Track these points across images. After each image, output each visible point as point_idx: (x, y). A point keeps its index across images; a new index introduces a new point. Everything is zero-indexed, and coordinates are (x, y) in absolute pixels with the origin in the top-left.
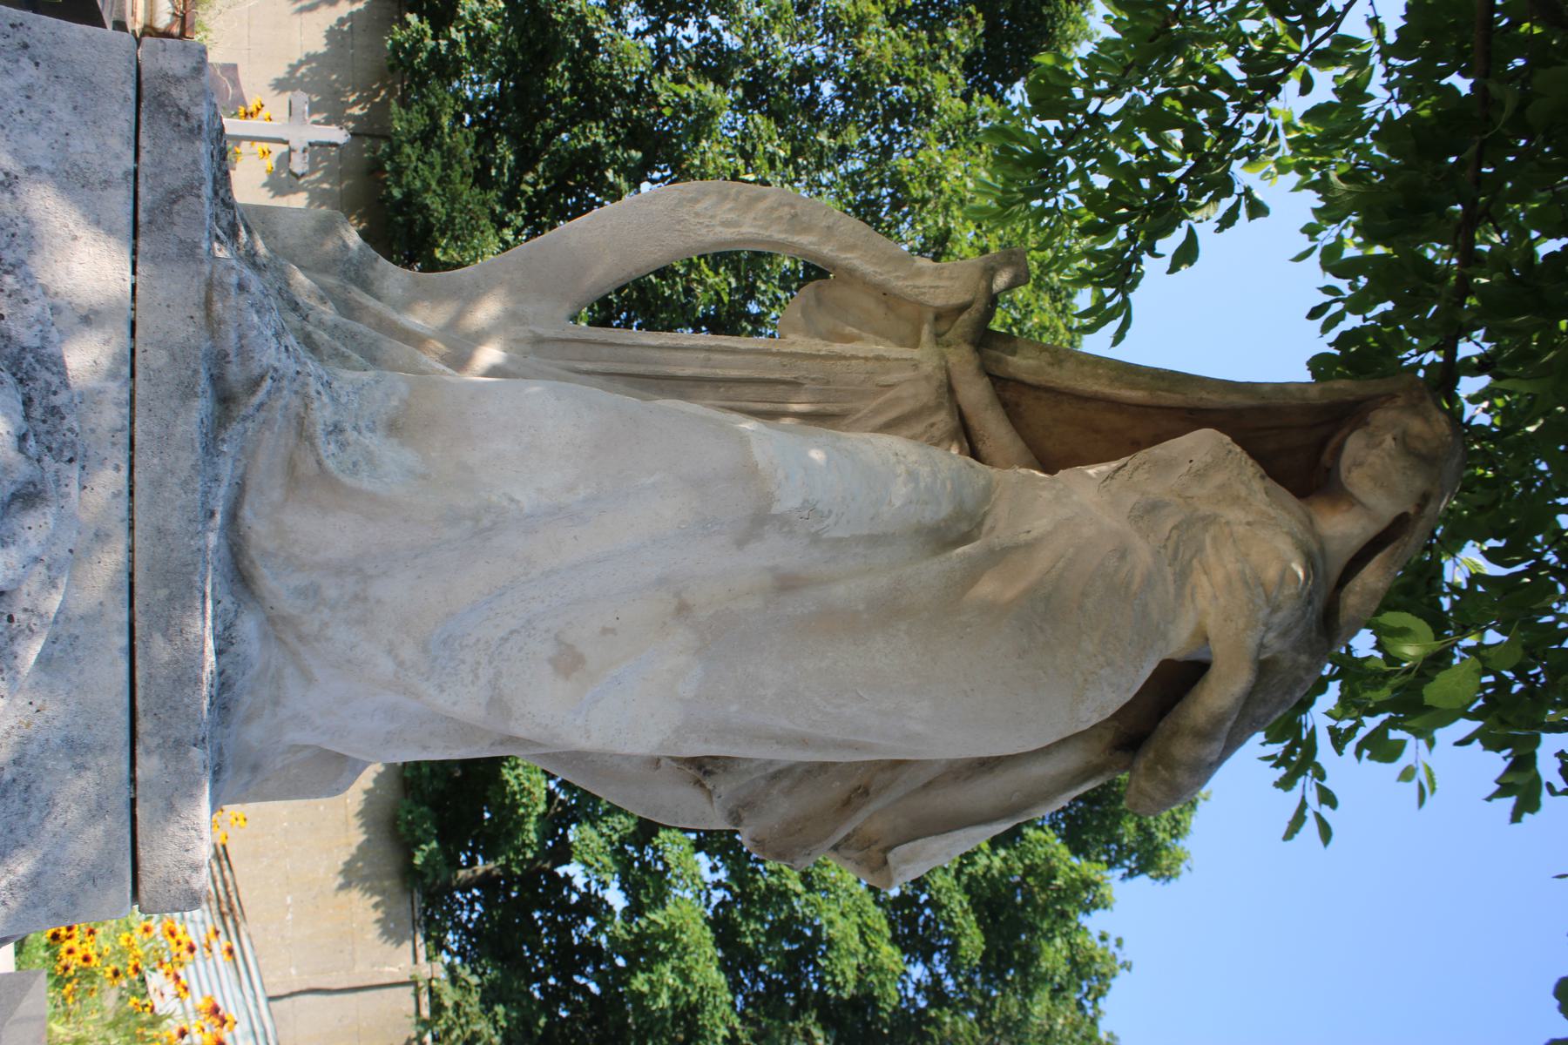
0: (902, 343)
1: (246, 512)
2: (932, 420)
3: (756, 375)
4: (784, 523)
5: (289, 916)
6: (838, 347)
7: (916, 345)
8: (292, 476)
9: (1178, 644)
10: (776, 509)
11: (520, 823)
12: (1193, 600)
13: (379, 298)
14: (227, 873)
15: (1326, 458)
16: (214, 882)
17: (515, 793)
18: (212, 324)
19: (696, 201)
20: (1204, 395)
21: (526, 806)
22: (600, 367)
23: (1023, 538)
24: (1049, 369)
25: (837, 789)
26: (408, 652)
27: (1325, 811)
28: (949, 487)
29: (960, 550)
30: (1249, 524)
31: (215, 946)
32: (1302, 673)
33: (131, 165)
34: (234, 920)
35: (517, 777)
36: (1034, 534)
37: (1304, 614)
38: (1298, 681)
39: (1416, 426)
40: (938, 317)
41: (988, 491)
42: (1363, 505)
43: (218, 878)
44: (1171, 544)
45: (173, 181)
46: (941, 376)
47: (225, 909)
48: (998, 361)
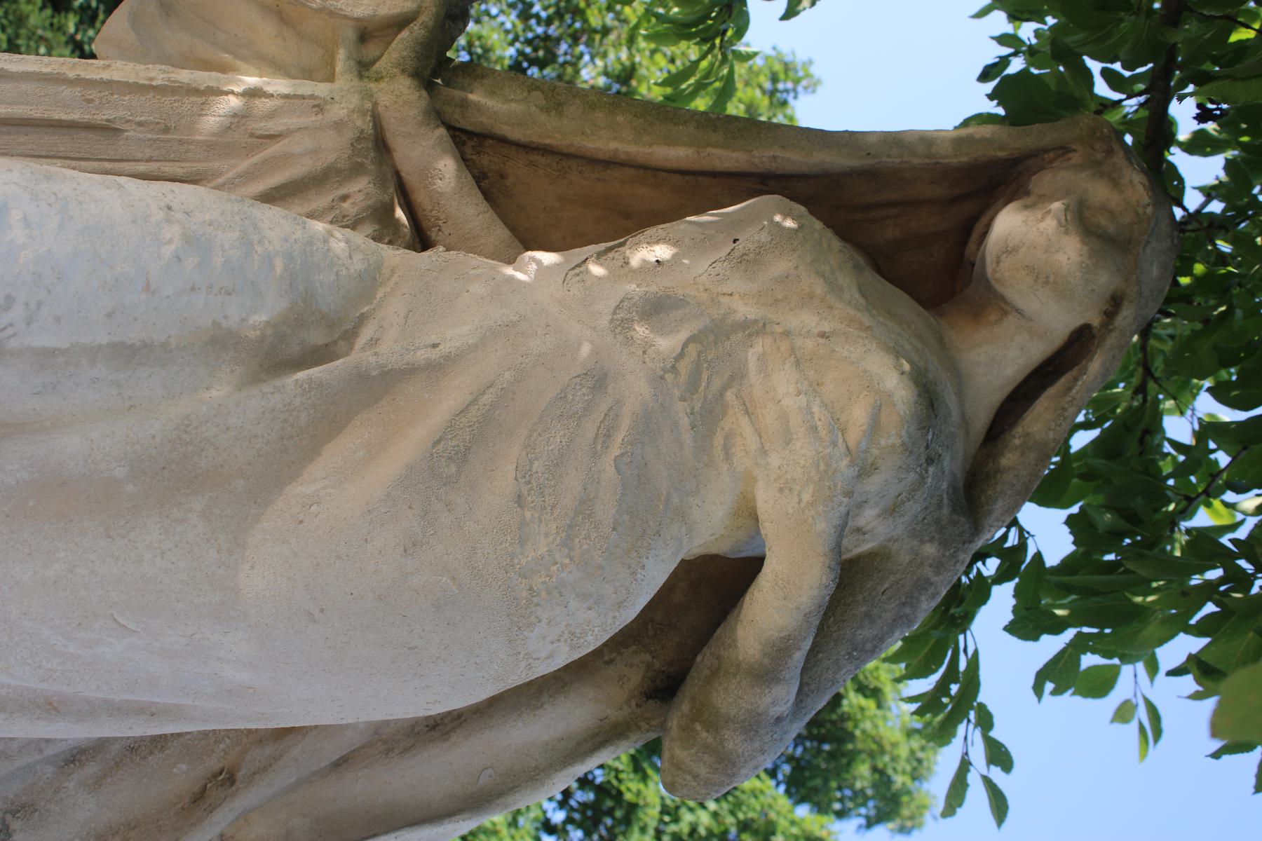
0: (308, 74)
2: (343, 191)
3: (36, 113)
6: (184, 76)
7: (331, 78)
9: (708, 530)
12: (728, 455)
15: (971, 247)
20: (779, 153)
23: (422, 355)
24: (543, 117)
25: (183, 776)
27: (996, 774)
28: (279, 264)
29: (301, 375)
30: (823, 335)
32: (928, 572)
36: (445, 348)
37: (922, 479)
38: (923, 585)
39: (1099, 192)
41: (369, 282)
42: (1018, 311)
44: (684, 367)
46: (366, 125)
48: (464, 105)
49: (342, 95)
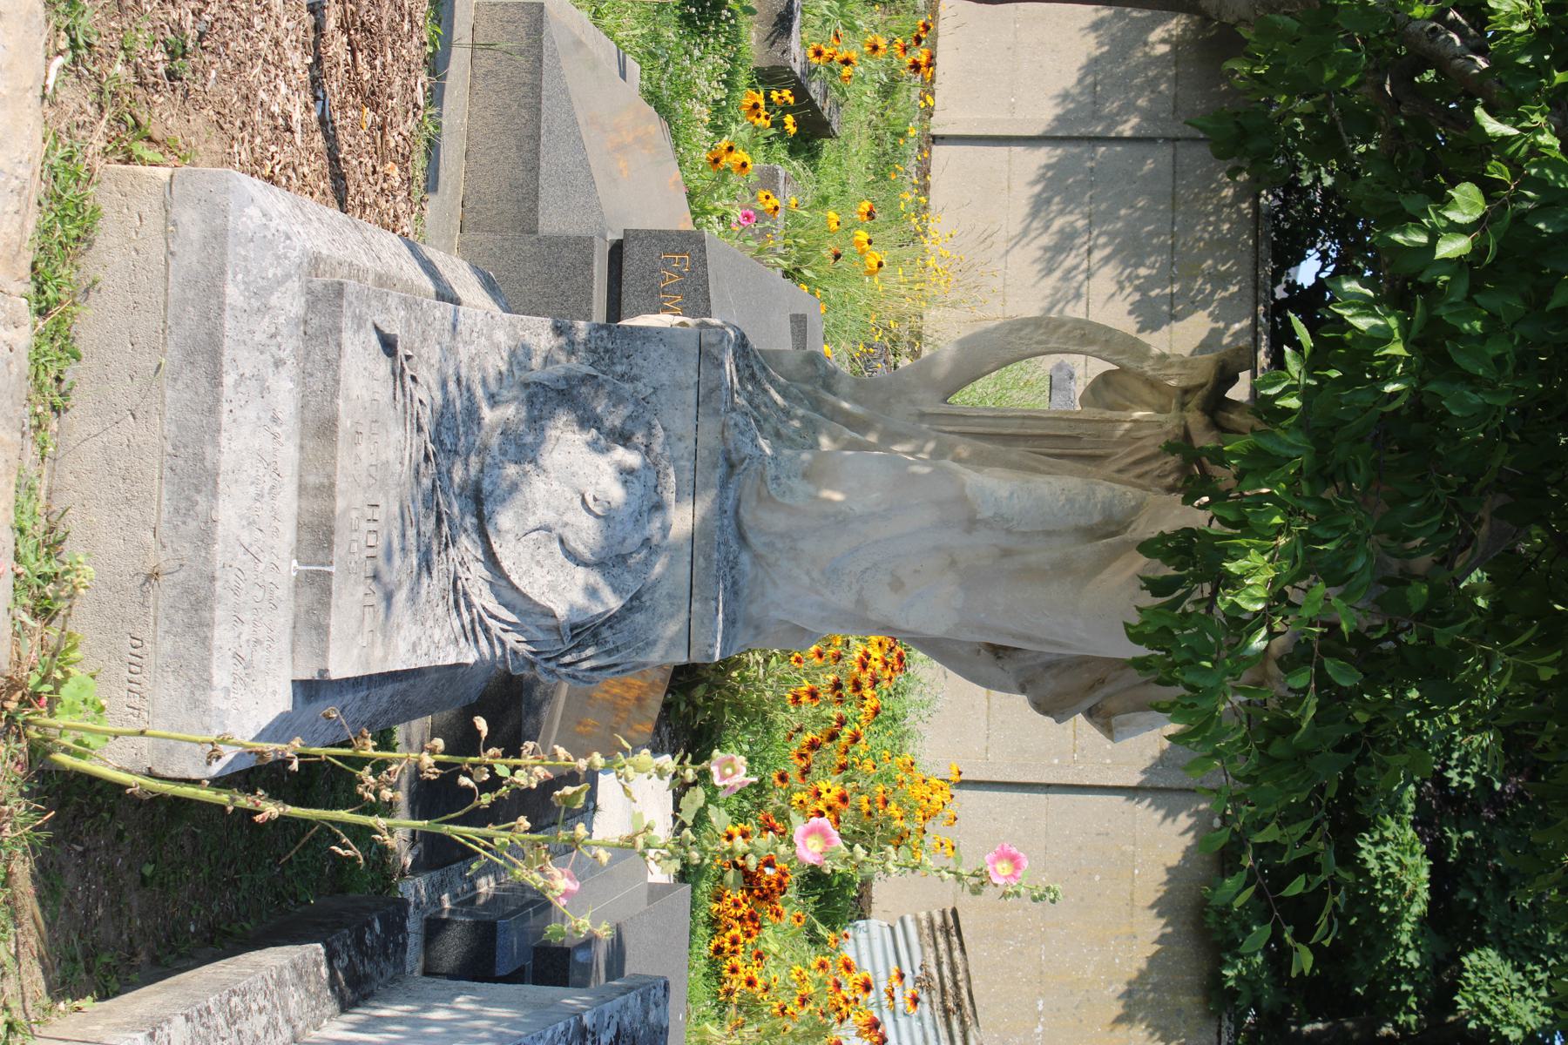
1: (742, 511)
4: (986, 523)
5: (1039, 1029)
8: (760, 499)
10: (979, 517)
11: (1384, 930)
13: (835, 394)
14: (957, 954)
16: (939, 964)
17: (1375, 880)
18: (724, 440)
19: (1020, 330)
21: (1391, 903)
22: (957, 429)
26: (816, 574)
31: (897, 994)
33: (696, 378)
34: (962, 1022)
35: (1380, 857)
40: (1186, 391)
43: (945, 959)
45: (712, 385)
46: (1180, 432)
47: (951, 1004)
49: (1171, 422)
